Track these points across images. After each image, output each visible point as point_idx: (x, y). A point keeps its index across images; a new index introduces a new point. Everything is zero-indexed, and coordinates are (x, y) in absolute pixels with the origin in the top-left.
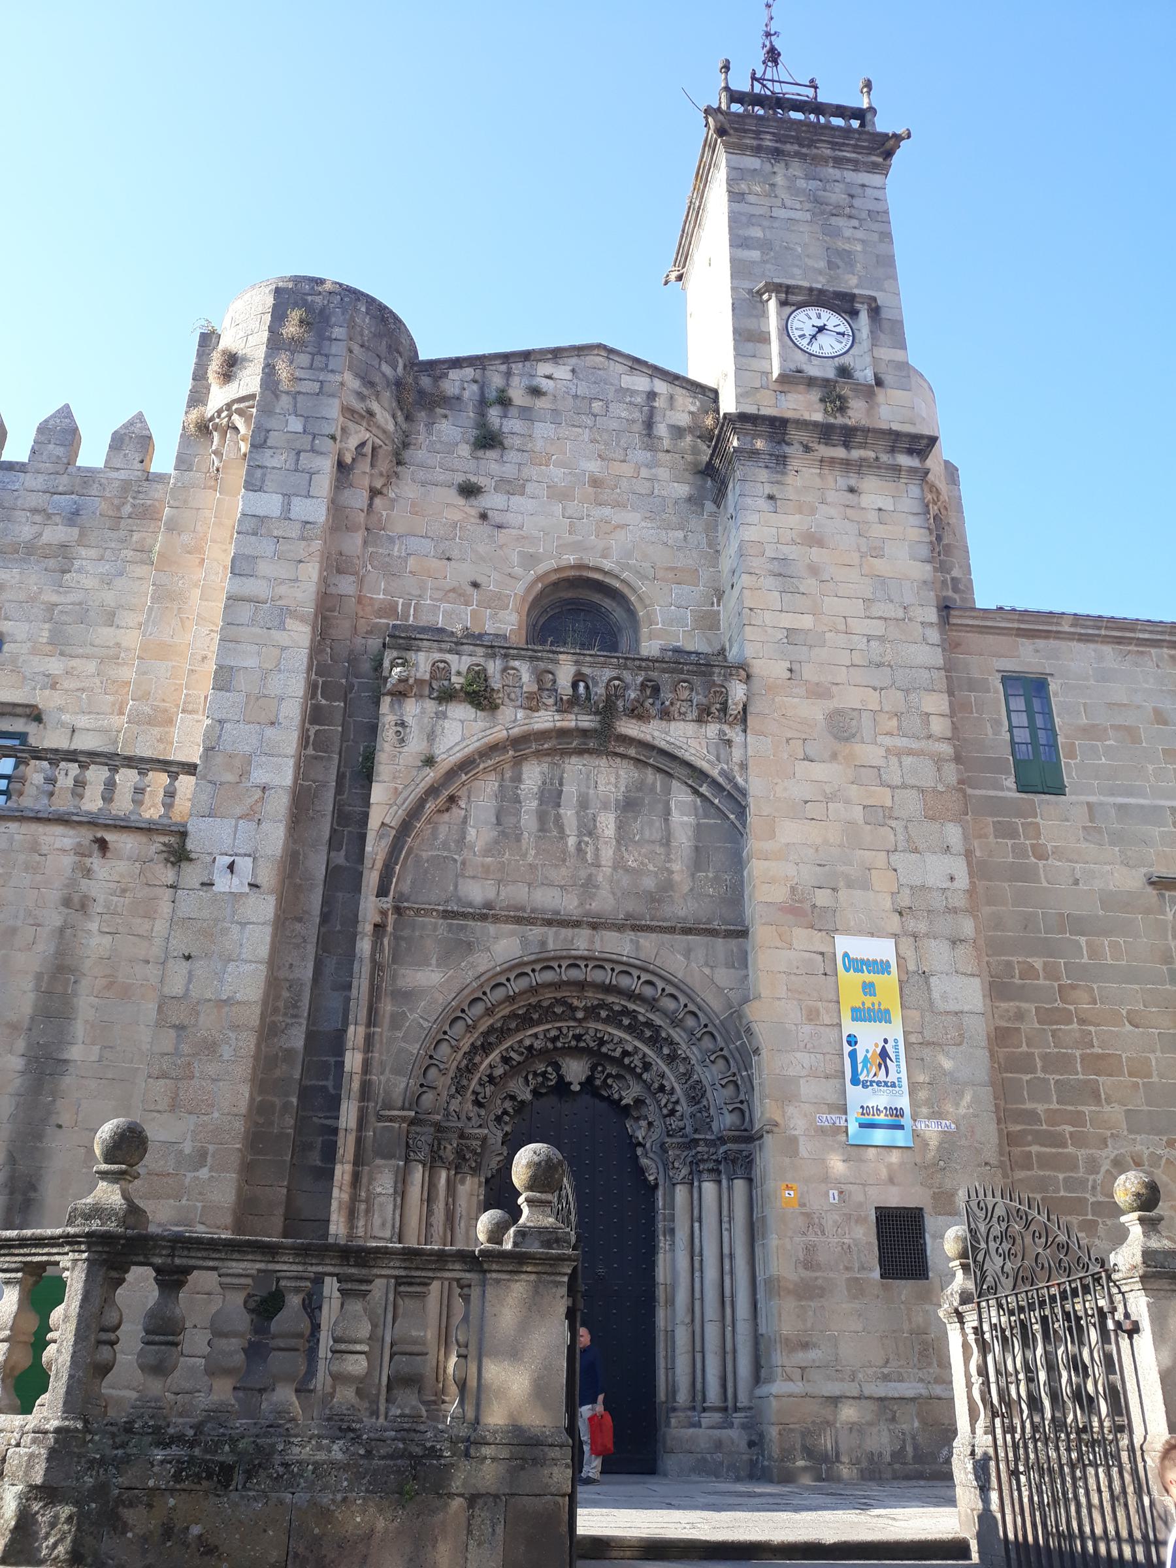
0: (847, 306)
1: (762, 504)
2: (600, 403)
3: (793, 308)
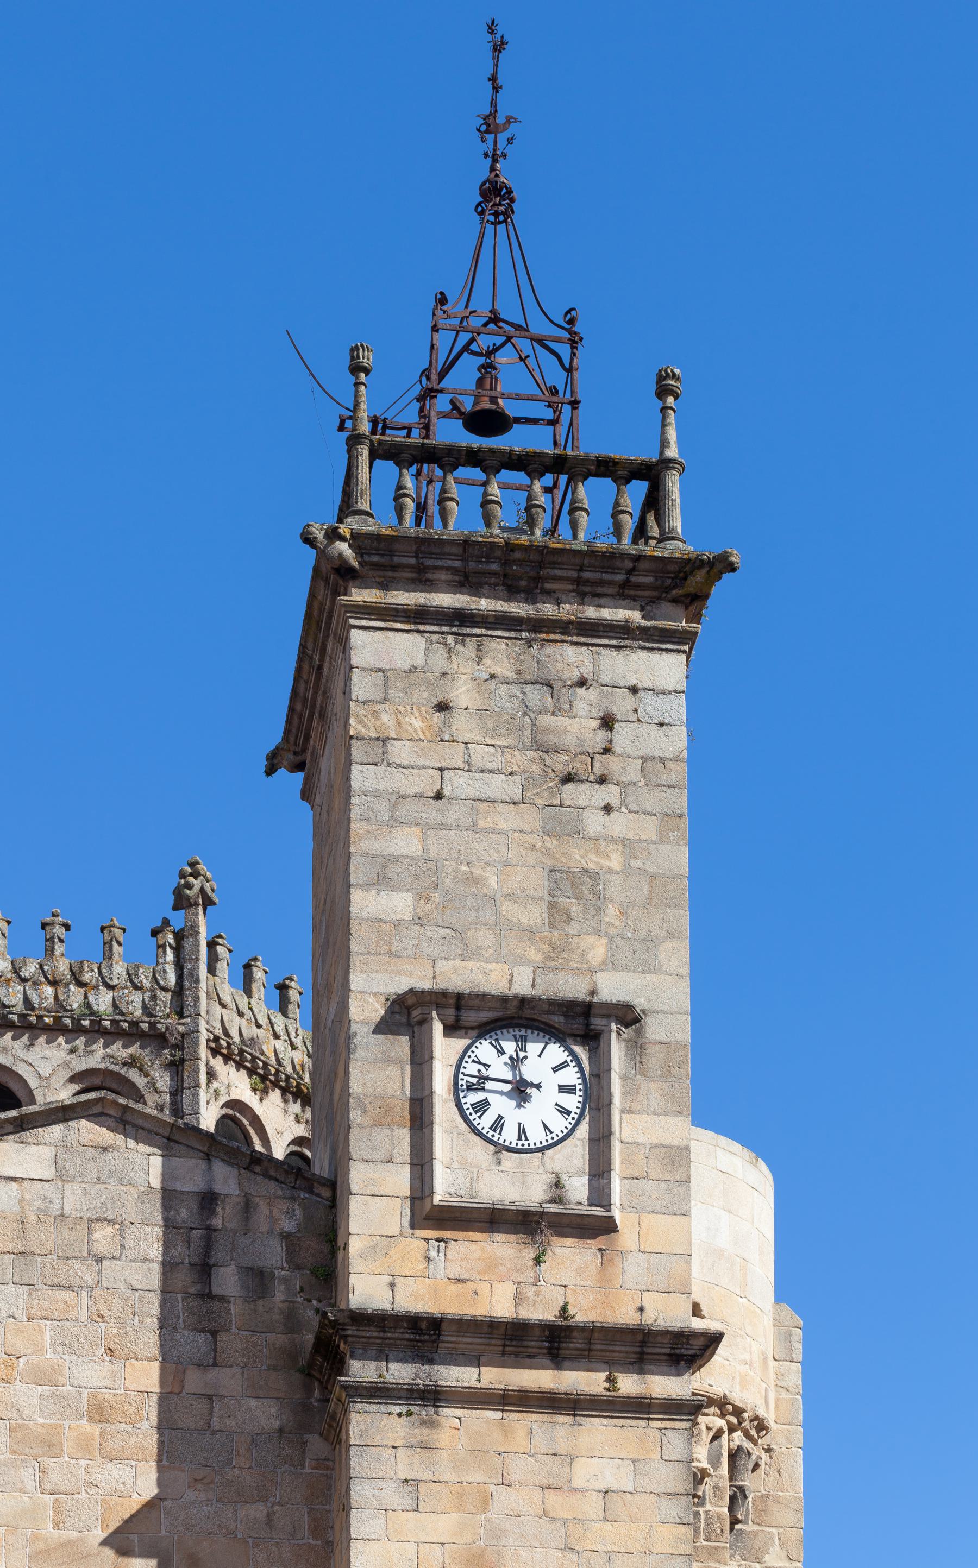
0: (577, 1026)
1: (392, 1495)
2: (109, 1230)
3: (474, 1033)
